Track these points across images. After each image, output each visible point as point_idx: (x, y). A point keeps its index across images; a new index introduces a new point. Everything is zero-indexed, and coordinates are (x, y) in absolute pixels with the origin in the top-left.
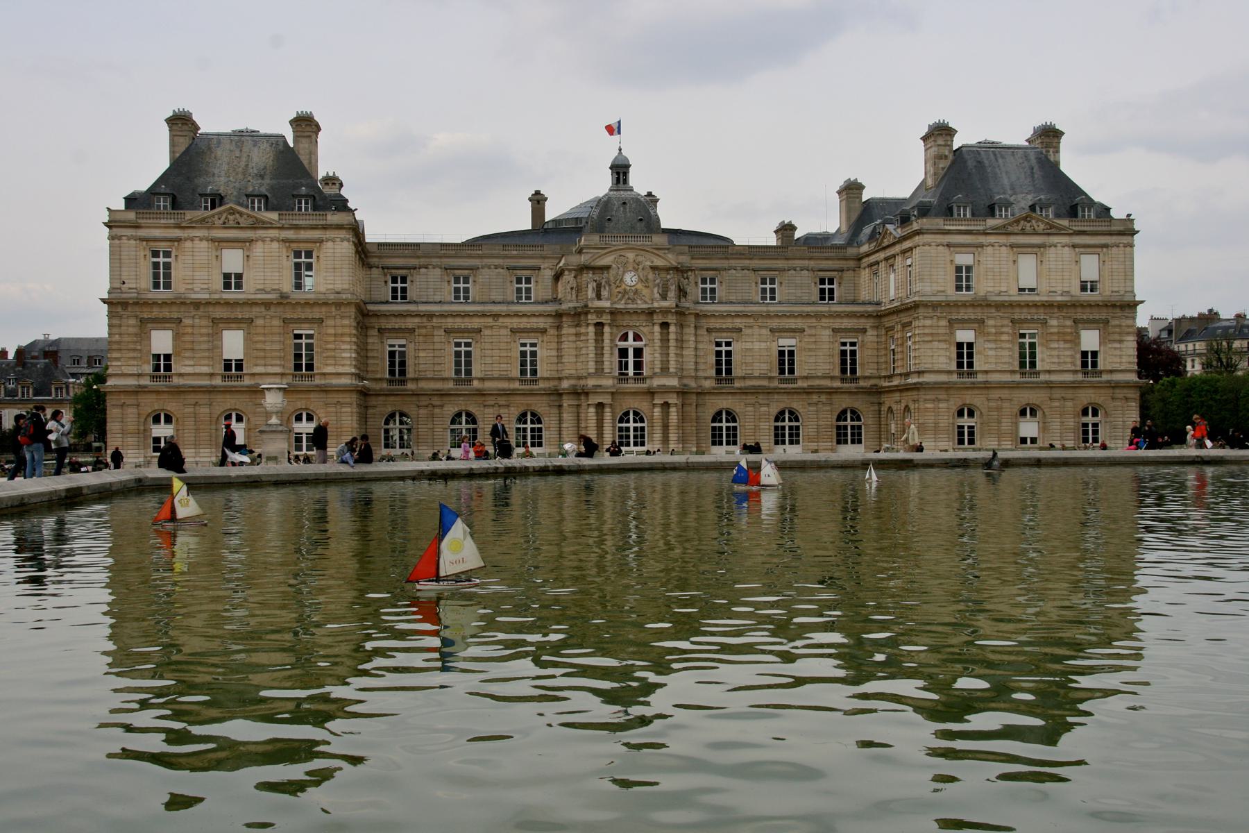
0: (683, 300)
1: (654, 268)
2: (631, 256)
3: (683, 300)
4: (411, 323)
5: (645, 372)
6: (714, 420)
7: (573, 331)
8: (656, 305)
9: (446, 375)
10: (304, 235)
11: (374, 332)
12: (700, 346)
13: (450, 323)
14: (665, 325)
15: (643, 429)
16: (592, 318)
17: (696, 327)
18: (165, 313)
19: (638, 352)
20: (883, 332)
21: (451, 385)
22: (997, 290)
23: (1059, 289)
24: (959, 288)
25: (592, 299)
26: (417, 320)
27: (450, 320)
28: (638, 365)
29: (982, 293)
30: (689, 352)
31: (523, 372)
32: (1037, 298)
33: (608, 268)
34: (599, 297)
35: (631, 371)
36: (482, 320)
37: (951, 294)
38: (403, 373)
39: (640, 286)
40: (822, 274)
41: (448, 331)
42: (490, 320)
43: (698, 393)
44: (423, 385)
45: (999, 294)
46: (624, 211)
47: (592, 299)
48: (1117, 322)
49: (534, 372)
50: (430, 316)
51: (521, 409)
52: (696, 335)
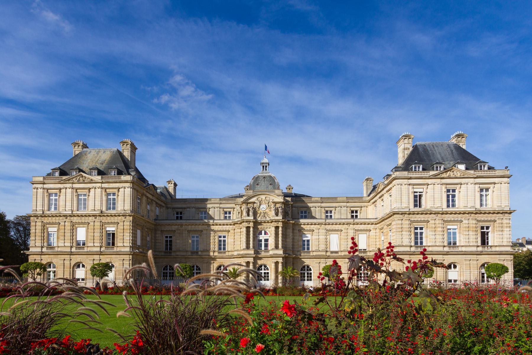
0: (287, 217)
1: (273, 202)
2: (263, 197)
3: (287, 217)
4: (174, 228)
5: (270, 248)
6: (302, 270)
7: (239, 230)
8: (273, 218)
9: (188, 249)
10: (112, 185)
11: (159, 232)
12: (296, 238)
13: (189, 228)
14: (277, 228)
15: (268, 273)
16: (246, 224)
17: (293, 229)
18: (54, 220)
19: (266, 240)
20: (378, 230)
21: (190, 254)
22: (436, 206)
23: (469, 206)
24: (415, 206)
25: (245, 216)
26: (176, 227)
27: (190, 227)
28: (266, 245)
29: (428, 207)
30: (289, 240)
31: (220, 249)
32: (457, 210)
33: (254, 203)
34: (248, 215)
35: (263, 248)
36: (203, 227)
37: (412, 208)
38: (171, 249)
39: (267, 211)
40: (352, 209)
41: (189, 231)
42: (206, 226)
43: (293, 258)
44: (178, 253)
45: (437, 208)
46: (264, 181)
47: (245, 216)
48: (500, 221)
49: (224, 249)
50: (182, 225)
51: (219, 264)
52: (293, 233)
